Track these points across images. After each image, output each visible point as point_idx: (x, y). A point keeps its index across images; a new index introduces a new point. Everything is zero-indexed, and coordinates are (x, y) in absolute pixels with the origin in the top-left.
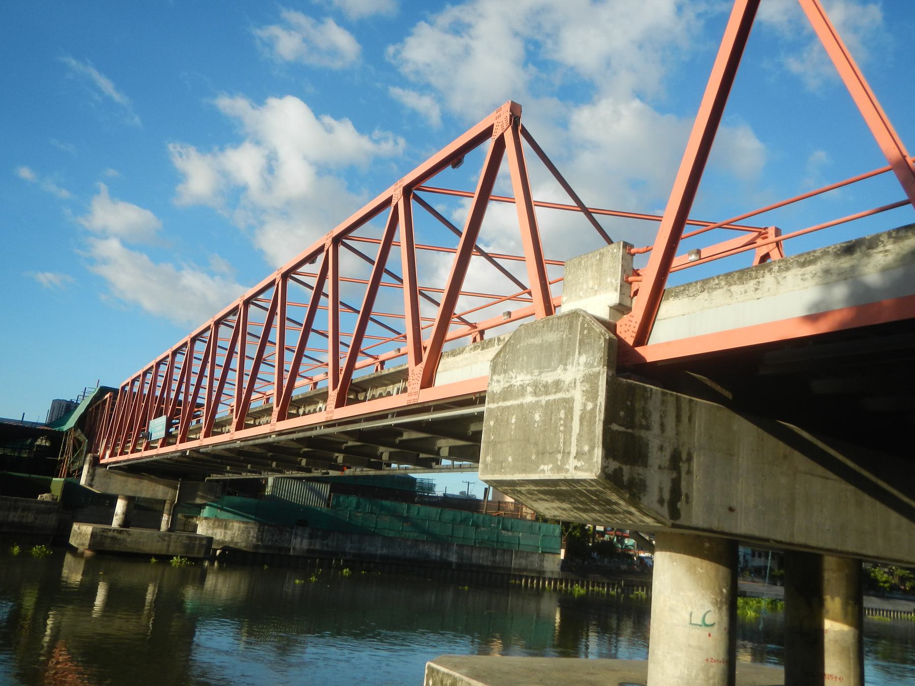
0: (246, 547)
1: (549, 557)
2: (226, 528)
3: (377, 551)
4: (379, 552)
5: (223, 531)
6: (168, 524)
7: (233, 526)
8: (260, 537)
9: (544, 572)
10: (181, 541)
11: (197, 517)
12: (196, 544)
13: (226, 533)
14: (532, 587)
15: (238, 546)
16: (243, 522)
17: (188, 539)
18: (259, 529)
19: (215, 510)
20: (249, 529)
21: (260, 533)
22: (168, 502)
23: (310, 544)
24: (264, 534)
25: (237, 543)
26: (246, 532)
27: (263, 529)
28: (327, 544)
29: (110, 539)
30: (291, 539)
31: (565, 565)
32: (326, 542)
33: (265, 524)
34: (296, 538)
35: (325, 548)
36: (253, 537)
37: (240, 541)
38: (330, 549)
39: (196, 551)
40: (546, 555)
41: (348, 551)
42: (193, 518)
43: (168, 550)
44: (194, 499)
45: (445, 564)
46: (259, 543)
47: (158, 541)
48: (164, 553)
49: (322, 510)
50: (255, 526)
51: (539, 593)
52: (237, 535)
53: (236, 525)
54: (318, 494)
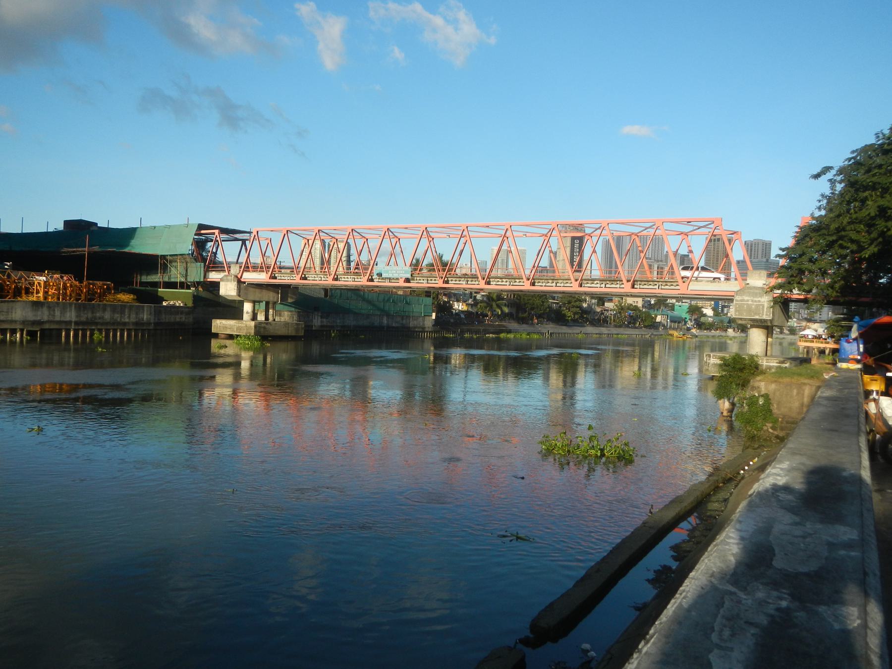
1: (427, 318)
9: (425, 328)
23: (322, 322)
28: (329, 321)
40: (426, 317)
43: (288, 333)
45: (390, 328)
48: (287, 334)
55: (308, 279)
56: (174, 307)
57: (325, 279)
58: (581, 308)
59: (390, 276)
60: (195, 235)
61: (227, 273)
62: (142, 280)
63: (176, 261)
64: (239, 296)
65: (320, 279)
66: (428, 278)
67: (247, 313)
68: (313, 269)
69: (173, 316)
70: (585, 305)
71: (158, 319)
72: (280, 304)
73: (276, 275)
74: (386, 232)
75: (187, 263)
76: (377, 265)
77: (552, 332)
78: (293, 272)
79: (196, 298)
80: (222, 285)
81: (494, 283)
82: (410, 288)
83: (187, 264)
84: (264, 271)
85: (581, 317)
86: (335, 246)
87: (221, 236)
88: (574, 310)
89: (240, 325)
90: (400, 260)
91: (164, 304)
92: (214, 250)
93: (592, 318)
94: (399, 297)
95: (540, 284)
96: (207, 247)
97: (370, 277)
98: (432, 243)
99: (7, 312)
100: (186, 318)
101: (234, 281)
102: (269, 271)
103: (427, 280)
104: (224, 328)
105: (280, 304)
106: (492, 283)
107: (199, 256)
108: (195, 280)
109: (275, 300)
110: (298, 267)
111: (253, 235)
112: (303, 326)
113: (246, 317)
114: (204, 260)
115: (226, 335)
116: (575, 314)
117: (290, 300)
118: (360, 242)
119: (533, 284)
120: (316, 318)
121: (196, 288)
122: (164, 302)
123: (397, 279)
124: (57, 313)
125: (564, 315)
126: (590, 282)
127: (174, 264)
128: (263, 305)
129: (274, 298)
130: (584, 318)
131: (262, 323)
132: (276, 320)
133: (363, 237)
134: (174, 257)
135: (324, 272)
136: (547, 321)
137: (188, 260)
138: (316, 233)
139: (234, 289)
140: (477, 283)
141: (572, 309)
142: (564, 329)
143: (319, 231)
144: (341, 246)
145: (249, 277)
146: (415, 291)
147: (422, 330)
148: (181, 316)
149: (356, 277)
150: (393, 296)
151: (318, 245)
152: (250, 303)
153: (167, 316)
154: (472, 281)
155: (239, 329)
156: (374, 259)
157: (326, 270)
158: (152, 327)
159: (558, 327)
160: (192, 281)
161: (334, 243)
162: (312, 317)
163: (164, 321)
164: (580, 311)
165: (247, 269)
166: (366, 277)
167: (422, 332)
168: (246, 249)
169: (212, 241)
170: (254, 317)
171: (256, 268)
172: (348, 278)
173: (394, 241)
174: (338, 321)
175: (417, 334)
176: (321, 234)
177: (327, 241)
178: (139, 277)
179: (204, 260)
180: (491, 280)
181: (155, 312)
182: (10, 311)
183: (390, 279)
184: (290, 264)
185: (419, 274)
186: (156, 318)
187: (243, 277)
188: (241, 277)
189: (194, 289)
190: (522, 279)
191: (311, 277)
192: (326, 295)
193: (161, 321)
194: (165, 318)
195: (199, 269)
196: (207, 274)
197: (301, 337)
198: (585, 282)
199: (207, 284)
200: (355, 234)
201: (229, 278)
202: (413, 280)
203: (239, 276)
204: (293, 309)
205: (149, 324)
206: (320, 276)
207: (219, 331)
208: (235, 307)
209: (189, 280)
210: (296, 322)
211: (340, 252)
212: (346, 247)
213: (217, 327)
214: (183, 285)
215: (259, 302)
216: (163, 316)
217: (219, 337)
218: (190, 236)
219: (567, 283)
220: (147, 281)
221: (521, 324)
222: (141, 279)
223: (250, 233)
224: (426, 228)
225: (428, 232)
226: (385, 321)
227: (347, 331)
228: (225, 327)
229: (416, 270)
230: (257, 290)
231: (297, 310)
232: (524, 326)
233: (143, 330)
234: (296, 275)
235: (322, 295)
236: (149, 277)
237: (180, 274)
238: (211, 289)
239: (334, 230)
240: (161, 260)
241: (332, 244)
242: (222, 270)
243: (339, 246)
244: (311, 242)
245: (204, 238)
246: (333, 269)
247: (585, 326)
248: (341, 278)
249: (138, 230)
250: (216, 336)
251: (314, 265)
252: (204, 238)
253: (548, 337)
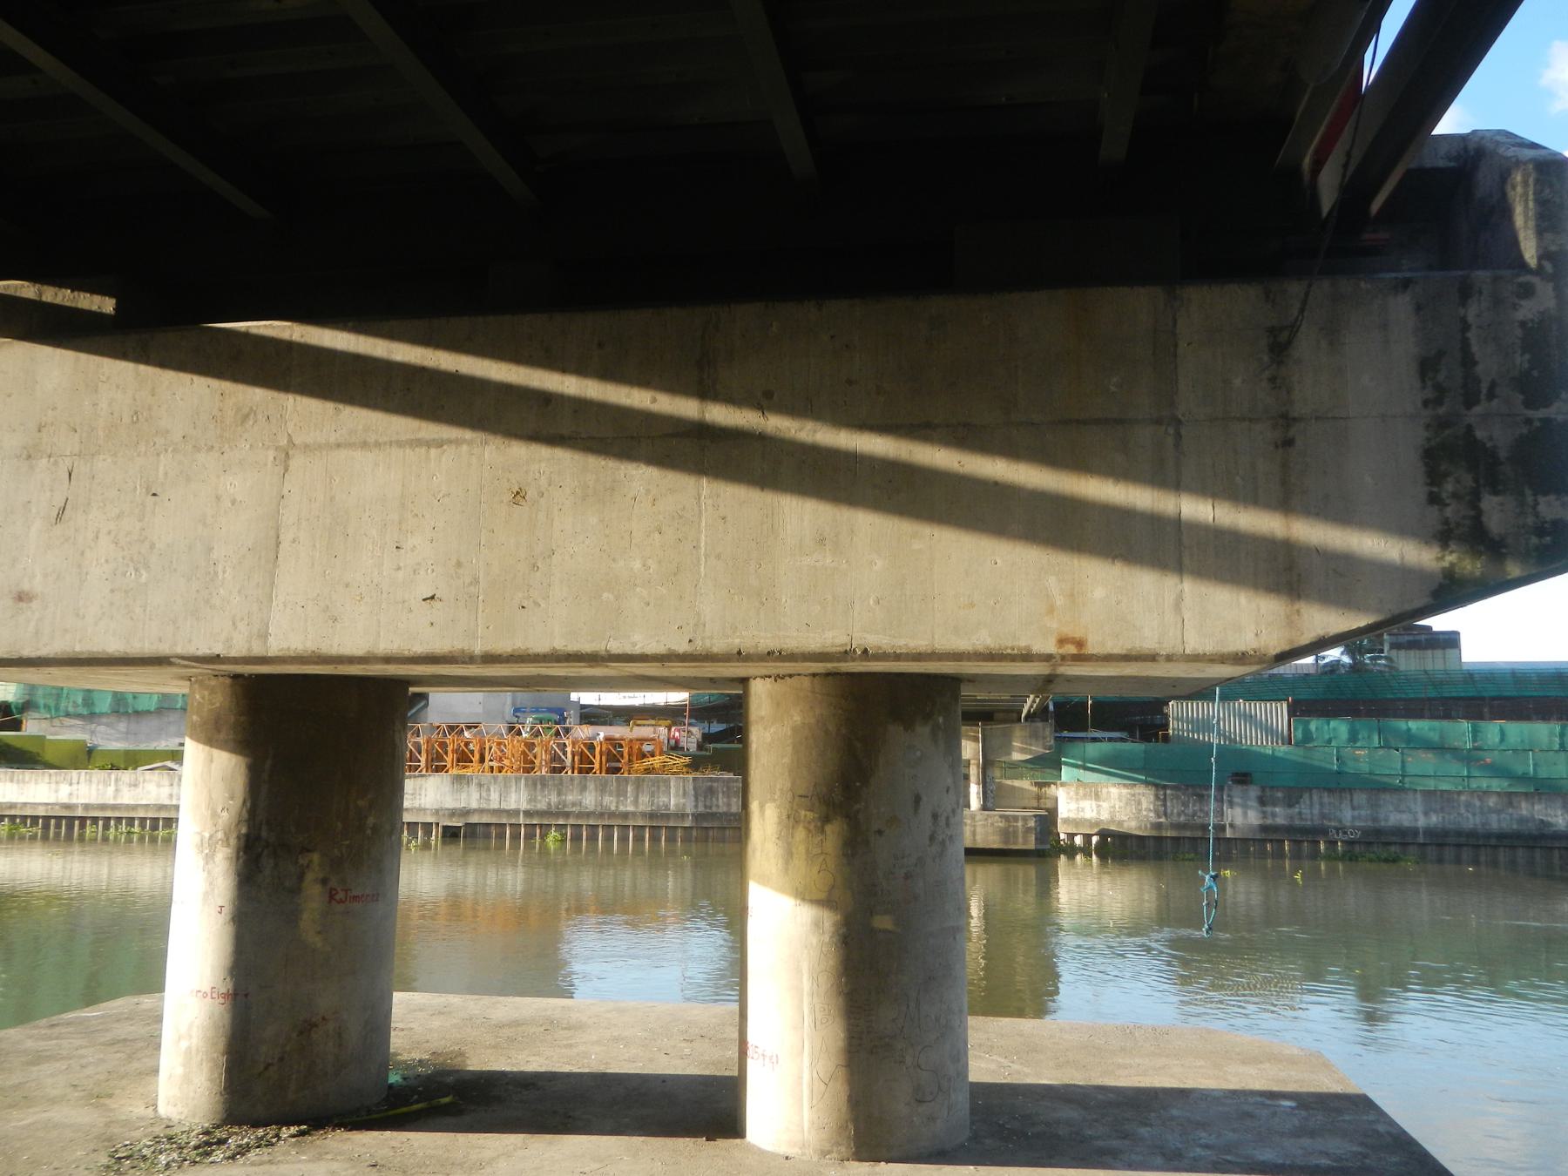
0: (1140, 828)
2: (1097, 797)
6: (979, 798)
7: (1108, 793)
10: (992, 824)
11: (1055, 784)
15: (1126, 825)
16: (1125, 785)
17: (1003, 821)
18: (1157, 797)
19: (1075, 770)
20: (1137, 799)
21: (1160, 803)
22: (972, 762)
23: (1264, 813)
24: (1168, 804)
25: (1120, 823)
26: (1133, 802)
27: (1165, 795)
28: (1300, 813)
30: (1222, 809)
32: (1297, 810)
33: (1165, 787)
37: (1126, 818)
39: (1020, 840)
42: (1049, 786)
44: (1010, 754)
46: (1162, 820)
49: (1277, 754)
52: (1119, 808)
53: (1114, 791)
54: (1269, 730)
99: (412, 794)
124: (494, 796)
182: (418, 792)
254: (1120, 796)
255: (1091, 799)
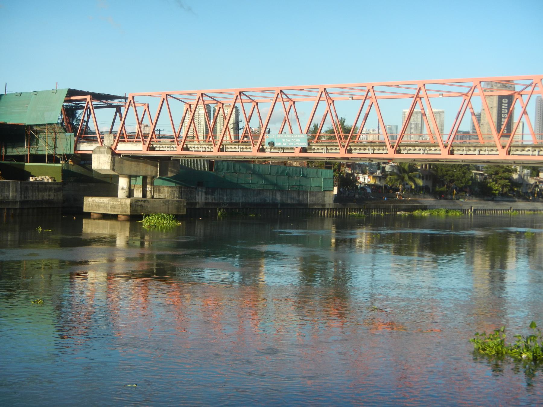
3: (240, 200)
4: (241, 201)
5: (158, 194)
7: (164, 190)
8: (180, 196)
10: (174, 204)
12: (181, 205)
13: (160, 195)
14: (333, 215)
16: (171, 187)
18: (179, 191)
24: (182, 194)
27: (182, 191)
29: (140, 207)
31: (337, 199)
34: (198, 196)
35: (214, 201)
36: (177, 197)
38: (216, 202)
39: (182, 210)
41: (225, 202)
47: (163, 205)
50: (177, 189)
51: (323, 219)
53: (166, 189)
55: (190, 149)
56: (41, 183)
57: (209, 150)
58: (510, 179)
59: (284, 145)
60: (65, 101)
61: (99, 144)
62: (7, 154)
63: (44, 132)
64: (114, 170)
65: (204, 149)
66: (328, 147)
67: (123, 189)
68: (196, 138)
69: (41, 193)
70: (515, 176)
71: (25, 197)
72: (159, 178)
73: (155, 146)
74: (278, 94)
75: (55, 133)
76: (269, 132)
77: (476, 208)
78: (173, 141)
79: (66, 173)
80: (94, 158)
81: (406, 152)
82: (307, 158)
83: (55, 135)
84: (141, 142)
85: (511, 190)
86: (221, 111)
87: (93, 103)
88: (503, 182)
89: (114, 203)
90: (296, 127)
91: (31, 180)
92: (86, 119)
93: (524, 191)
94: (294, 169)
95: (459, 152)
96: (77, 115)
97: (261, 147)
98: (332, 106)
100: (54, 195)
101: (108, 153)
102: (146, 141)
103: (327, 149)
104: (96, 207)
105: (158, 178)
106: (402, 152)
107: (69, 125)
108: (65, 153)
109: (154, 174)
110: (178, 136)
111: (128, 101)
112: (185, 204)
113: (122, 193)
114: (74, 129)
115: (98, 215)
116: (503, 186)
117: (170, 174)
118: (249, 107)
119: (452, 152)
120: (200, 193)
121: (66, 161)
122: (31, 178)
123: (292, 148)
125: (491, 189)
126: (520, 149)
127: (42, 135)
128: (140, 180)
129: (152, 171)
130: (514, 191)
131: (139, 200)
132: (155, 197)
133: (253, 100)
134: (42, 127)
135: (208, 142)
136: (470, 195)
137: (57, 130)
138: (199, 97)
139: (108, 162)
140: (385, 151)
141: (499, 182)
142: (491, 205)
143: (202, 94)
144: (228, 111)
145: (124, 148)
146: (314, 162)
147: (322, 207)
148: (50, 193)
149: (244, 147)
150: (288, 168)
151: (201, 110)
152: (125, 178)
153: (34, 193)
154: (379, 150)
155: (113, 207)
156: (265, 125)
157: (211, 139)
158: (18, 206)
159: (483, 202)
160: (62, 153)
161: (220, 108)
162: (196, 193)
163: (31, 199)
164: (509, 184)
165: (121, 139)
166: (257, 147)
167: (321, 209)
168: (121, 117)
169: (83, 108)
170: (130, 194)
171: (132, 138)
172: (235, 148)
173: (288, 105)
174: (225, 198)
175: (315, 212)
176: (205, 98)
177: (212, 106)
178: (3, 150)
179: (74, 129)
180: (402, 148)
181: (21, 188)
183: (284, 148)
184: (168, 131)
185: (317, 142)
186: (23, 196)
187: (118, 148)
188: (115, 149)
189: (64, 162)
190: (438, 146)
191: (193, 147)
192: (211, 168)
193: (28, 199)
194: (33, 196)
195: (70, 139)
196: (78, 145)
197: (182, 216)
198: (515, 149)
199: (77, 157)
200: (243, 97)
201: (102, 149)
202: (311, 149)
203: (113, 148)
204: (174, 185)
205: (15, 202)
206: (204, 146)
207: (93, 210)
208: (109, 183)
209: (58, 153)
210: (177, 199)
211: (226, 119)
212: (234, 113)
213: (89, 204)
214: (51, 159)
215: (136, 177)
216: (30, 194)
217: (92, 217)
218: (59, 103)
219: (492, 150)
220: (13, 154)
221: (436, 198)
222: (6, 152)
223: (125, 98)
224: (325, 89)
225: (327, 93)
226: (278, 197)
227: (236, 209)
228: (98, 206)
229: (314, 137)
230: (133, 163)
231: (178, 185)
232: (442, 201)
233: (8, 209)
234: (176, 146)
235: (207, 165)
236: (15, 150)
237: (48, 146)
238: (83, 162)
239: (219, 93)
240: (28, 130)
241: (217, 109)
242: (94, 141)
243: (226, 112)
244: (193, 107)
245: (73, 105)
246: (219, 138)
247: (515, 201)
248: (228, 148)
249: (3, 97)
250: (88, 215)
251: (197, 134)
252: (73, 105)
253: (471, 214)
254: (168, 191)
255: (157, 193)
